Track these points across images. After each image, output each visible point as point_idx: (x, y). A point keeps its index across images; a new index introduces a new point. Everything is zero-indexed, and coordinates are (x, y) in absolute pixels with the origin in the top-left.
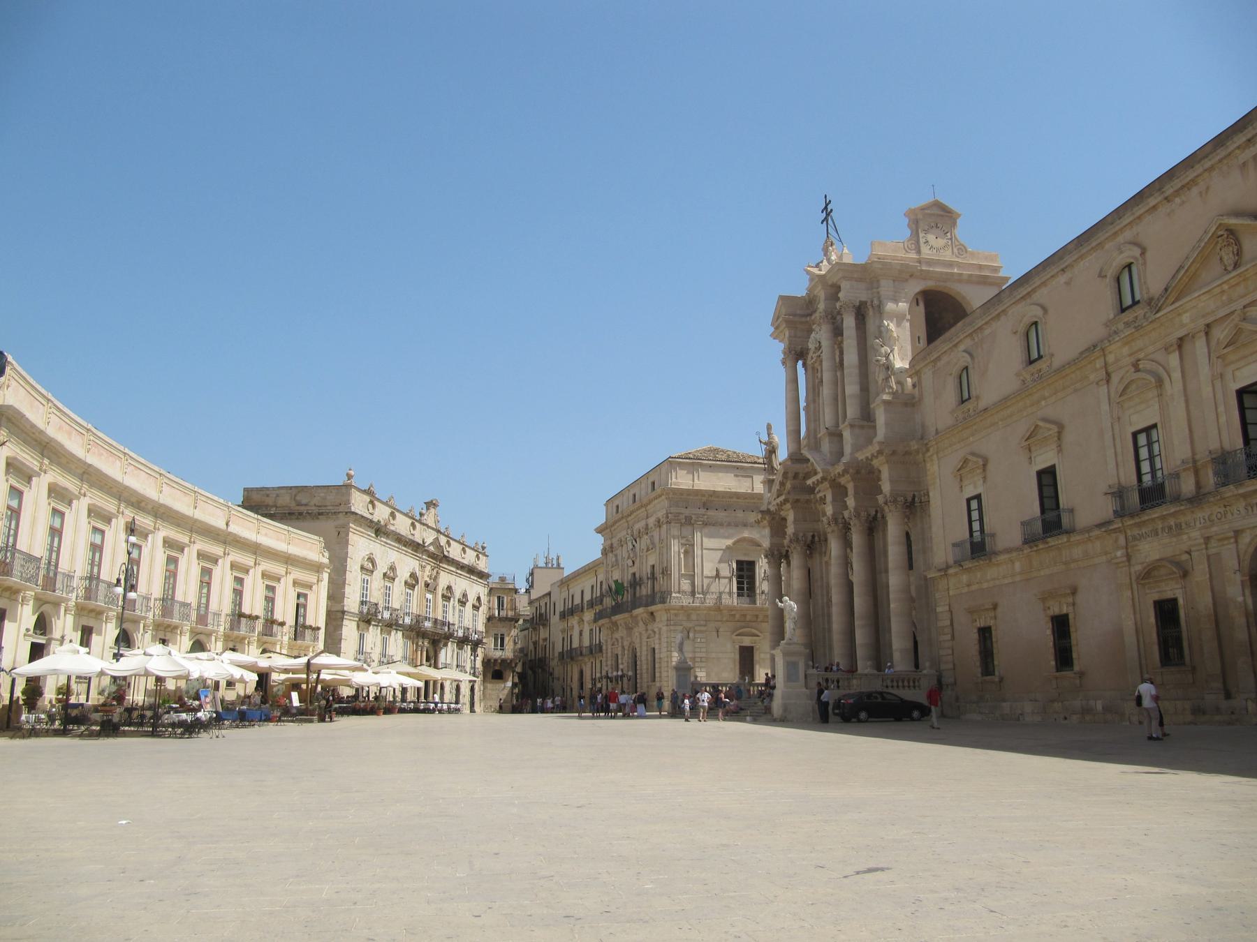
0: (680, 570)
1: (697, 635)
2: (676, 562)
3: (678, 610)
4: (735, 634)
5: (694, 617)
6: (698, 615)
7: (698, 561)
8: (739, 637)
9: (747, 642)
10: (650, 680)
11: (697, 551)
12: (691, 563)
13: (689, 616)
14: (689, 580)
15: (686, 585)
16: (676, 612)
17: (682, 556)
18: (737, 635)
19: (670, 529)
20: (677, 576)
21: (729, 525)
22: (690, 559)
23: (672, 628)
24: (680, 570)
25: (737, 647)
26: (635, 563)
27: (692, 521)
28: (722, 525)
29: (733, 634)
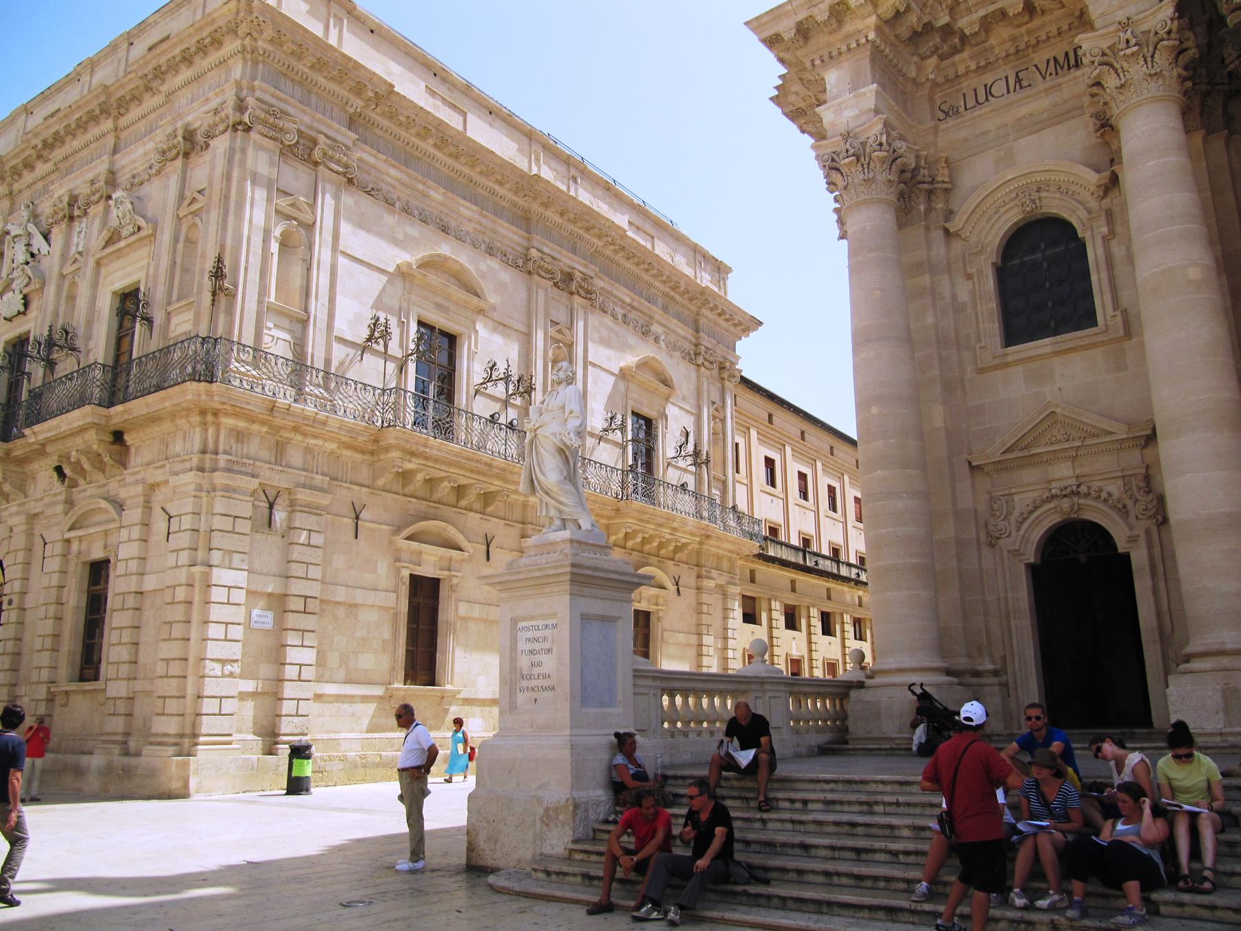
0: (263, 291)
1: (300, 520)
2: (255, 261)
3: (252, 419)
4: (407, 532)
5: (295, 456)
6: (308, 450)
7: (321, 280)
8: (415, 545)
9: (430, 562)
10: (64, 672)
11: (323, 253)
12: (297, 283)
13: (280, 448)
14: (290, 331)
15: (278, 342)
16: (242, 424)
17: (275, 247)
18: (408, 538)
19: (244, 151)
20: (252, 306)
21: (407, 210)
22: (297, 270)
23: (220, 479)
24: (263, 291)
25: (406, 573)
26: (34, 305)
27: (317, 154)
28: (389, 203)
29: (398, 530)
